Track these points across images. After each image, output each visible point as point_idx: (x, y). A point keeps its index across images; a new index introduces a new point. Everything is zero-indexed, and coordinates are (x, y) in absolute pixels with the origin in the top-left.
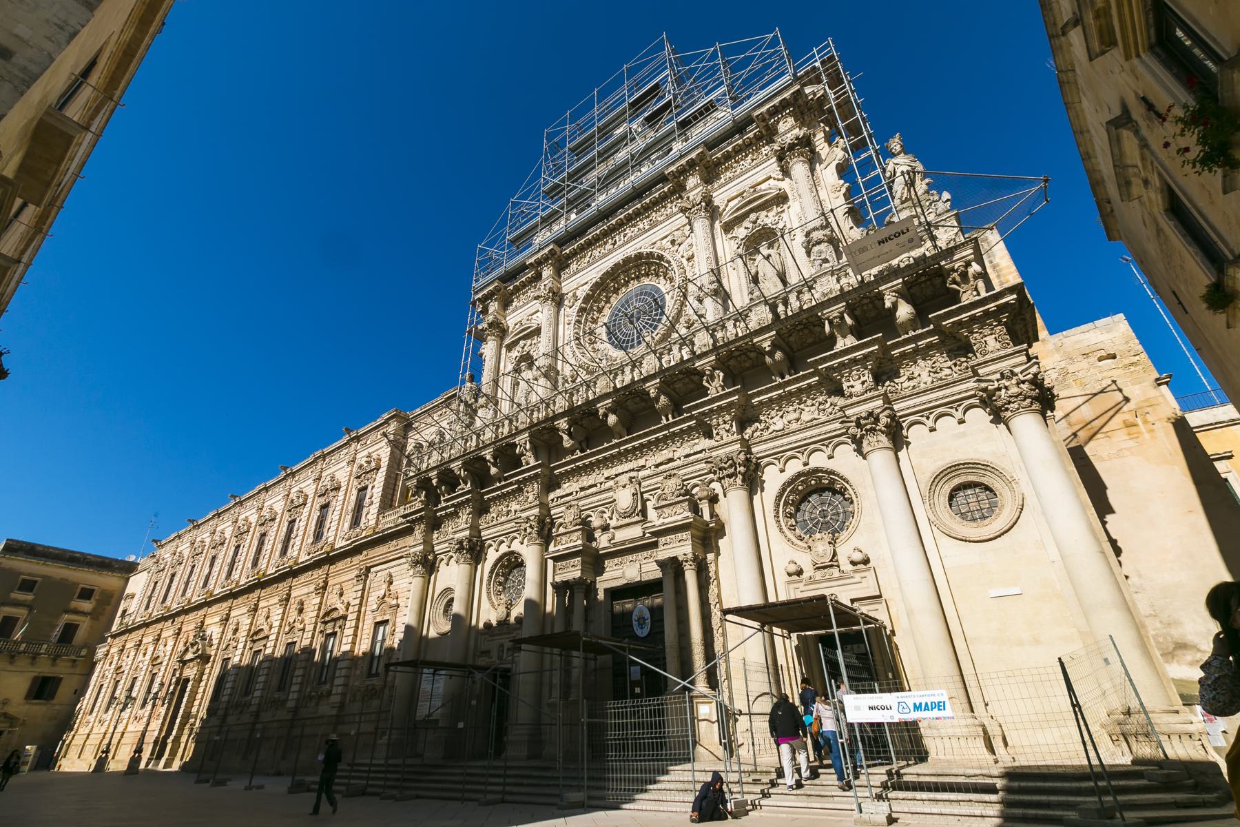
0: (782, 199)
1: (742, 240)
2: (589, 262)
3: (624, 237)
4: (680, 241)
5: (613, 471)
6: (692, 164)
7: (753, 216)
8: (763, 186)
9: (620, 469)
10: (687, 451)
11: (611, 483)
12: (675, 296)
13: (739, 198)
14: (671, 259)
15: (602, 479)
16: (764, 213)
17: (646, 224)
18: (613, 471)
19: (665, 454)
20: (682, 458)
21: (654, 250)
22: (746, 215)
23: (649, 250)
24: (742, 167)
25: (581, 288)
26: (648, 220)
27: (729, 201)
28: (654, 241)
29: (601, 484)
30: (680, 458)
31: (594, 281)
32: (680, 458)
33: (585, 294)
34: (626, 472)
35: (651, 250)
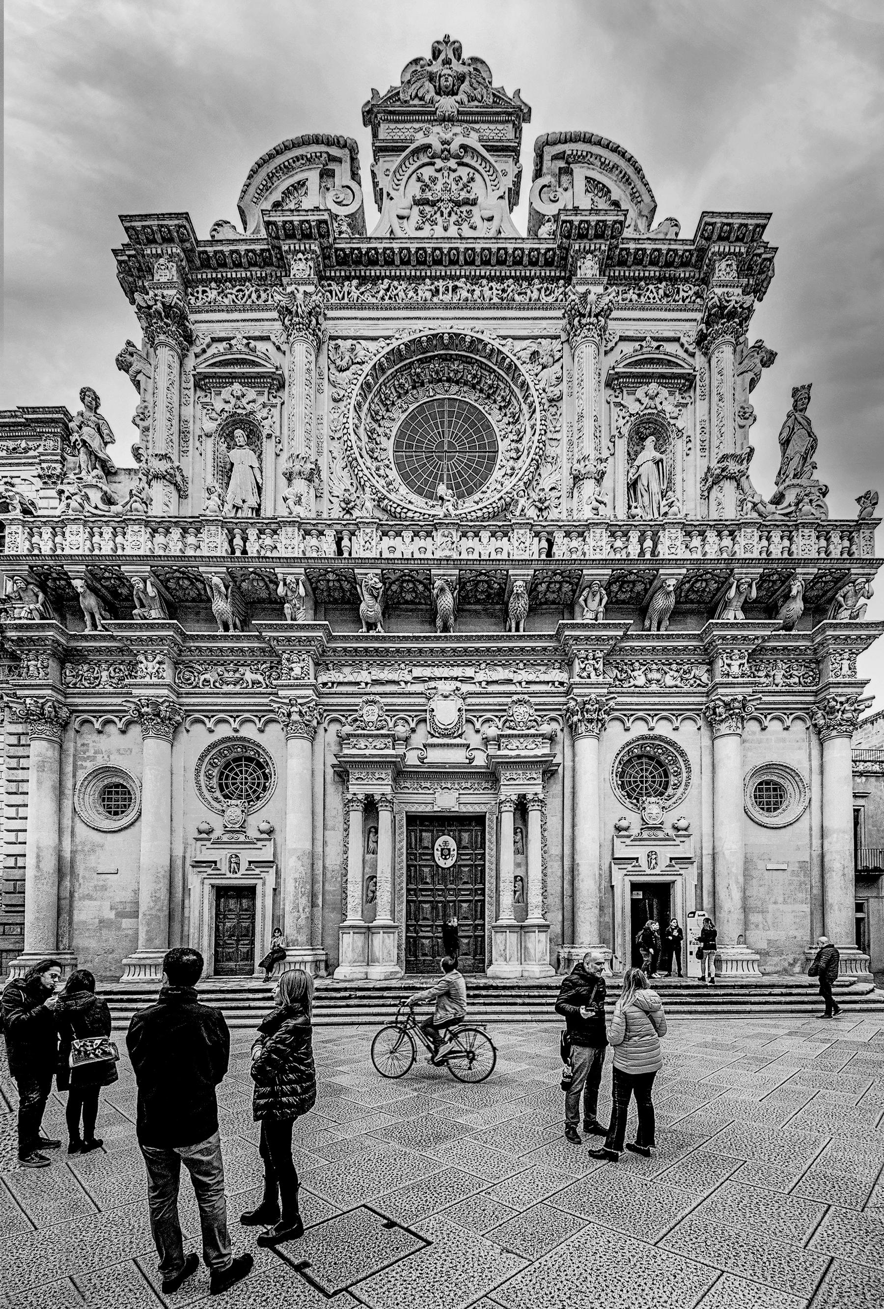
0: (687, 383)
1: (631, 415)
2: (383, 299)
5: (427, 672)
7: (653, 387)
8: (671, 348)
9: (439, 672)
10: (532, 677)
11: (419, 688)
12: (532, 451)
14: (531, 385)
15: (409, 678)
18: (427, 672)
19: (501, 674)
20: (524, 684)
22: (646, 378)
29: (406, 683)
30: (520, 683)
31: (395, 344)
32: (520, 683)
33: (376, 359)
34: (446, 679)
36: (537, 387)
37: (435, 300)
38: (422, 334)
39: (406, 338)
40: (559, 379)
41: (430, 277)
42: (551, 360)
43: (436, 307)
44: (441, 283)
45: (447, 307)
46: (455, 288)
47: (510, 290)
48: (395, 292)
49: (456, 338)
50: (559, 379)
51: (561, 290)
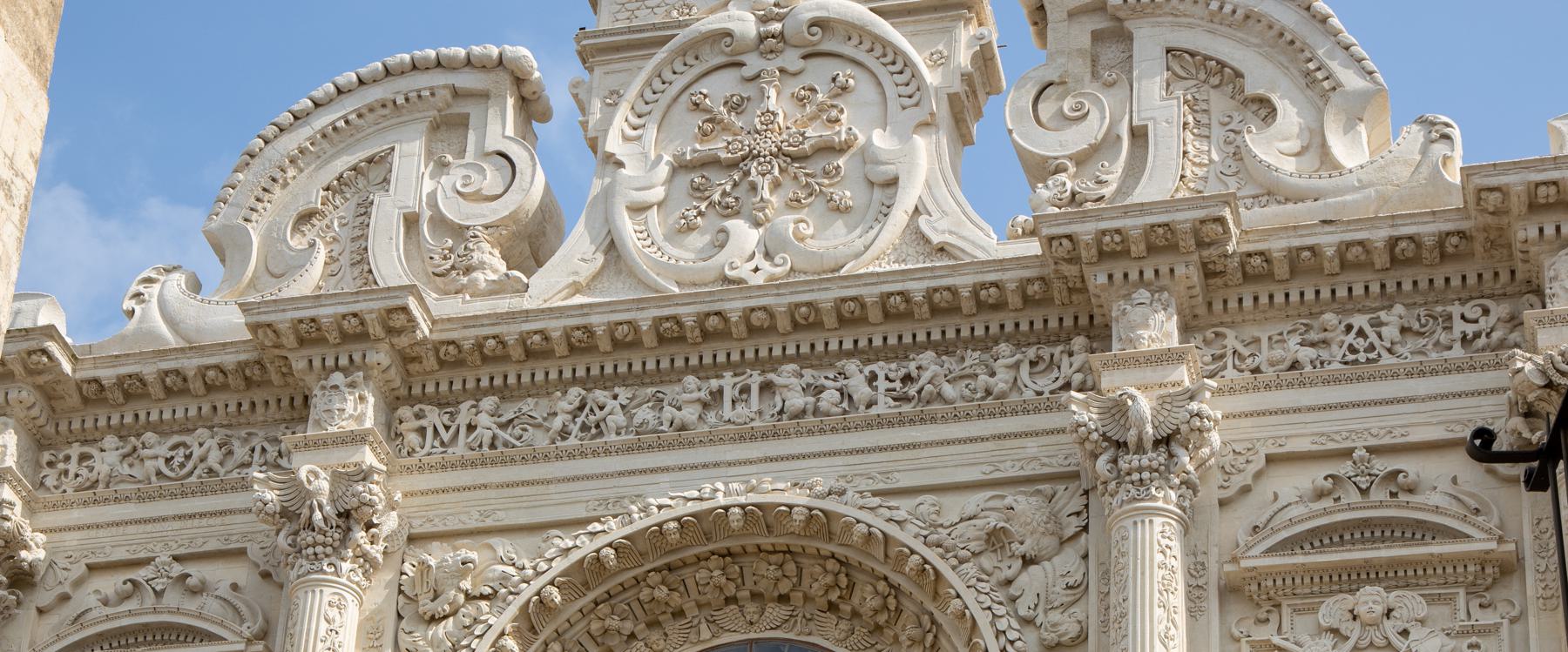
2: (564, 434)
3: (767, 388)
4: (1027, 548)
6: (1162, 241)
7: (1371, 598)
13: (1316, 475)
14: (983, 620)
16: (1410, 603)
17: (882, 384)
21: (904, 536)
22: (1352, 578)
23: (879, 524)
24: (1360, 344)
25: (503, 546)
26: (895, 369)
27: (1271, 460)
28: (905, 481)
31: (586, 546)
33: (528, 591)
35: (893, 530)
36: (1002, 624)
37: (711, 417)
38: (665, 514)
39: (616, 530)
40: (1078, 589)
41: (695, 371)
42: (1049, 542)
43: (713, 440)
44: (728, 381)
45: (747, 436)
46: (767, 388)
47: (926, 376)
48: (600, 414)
49: (762, 516)
50: (1078, 589)
51: (1078, 360)
